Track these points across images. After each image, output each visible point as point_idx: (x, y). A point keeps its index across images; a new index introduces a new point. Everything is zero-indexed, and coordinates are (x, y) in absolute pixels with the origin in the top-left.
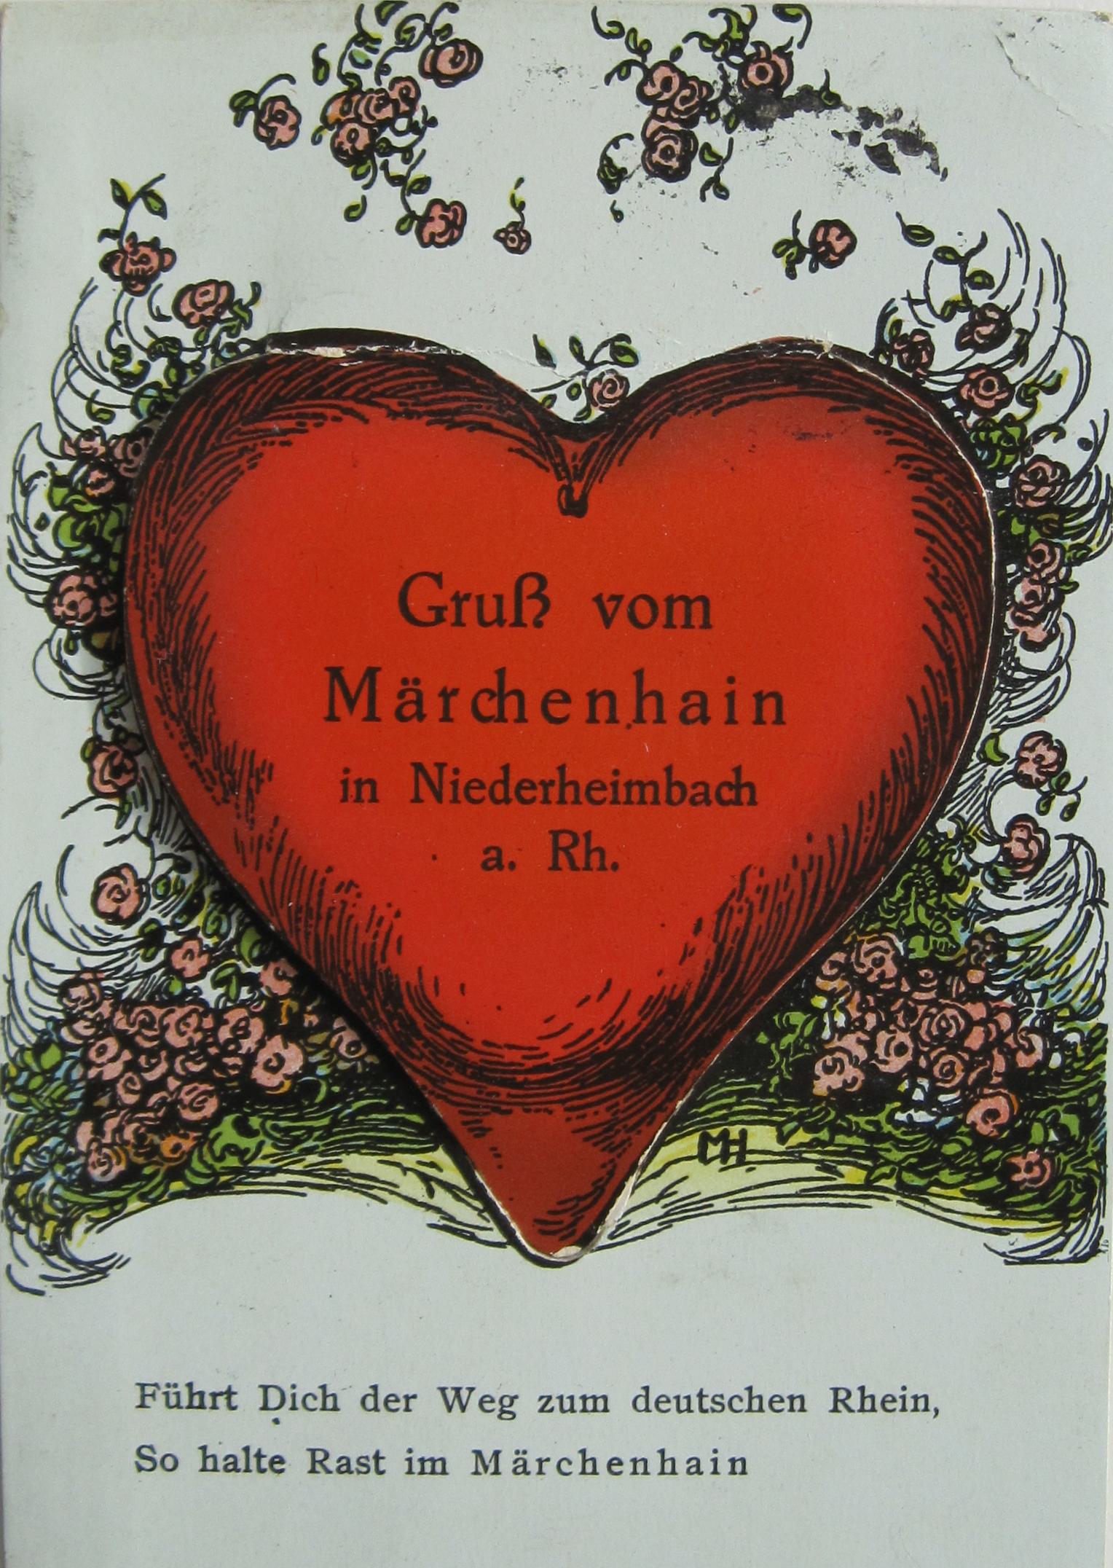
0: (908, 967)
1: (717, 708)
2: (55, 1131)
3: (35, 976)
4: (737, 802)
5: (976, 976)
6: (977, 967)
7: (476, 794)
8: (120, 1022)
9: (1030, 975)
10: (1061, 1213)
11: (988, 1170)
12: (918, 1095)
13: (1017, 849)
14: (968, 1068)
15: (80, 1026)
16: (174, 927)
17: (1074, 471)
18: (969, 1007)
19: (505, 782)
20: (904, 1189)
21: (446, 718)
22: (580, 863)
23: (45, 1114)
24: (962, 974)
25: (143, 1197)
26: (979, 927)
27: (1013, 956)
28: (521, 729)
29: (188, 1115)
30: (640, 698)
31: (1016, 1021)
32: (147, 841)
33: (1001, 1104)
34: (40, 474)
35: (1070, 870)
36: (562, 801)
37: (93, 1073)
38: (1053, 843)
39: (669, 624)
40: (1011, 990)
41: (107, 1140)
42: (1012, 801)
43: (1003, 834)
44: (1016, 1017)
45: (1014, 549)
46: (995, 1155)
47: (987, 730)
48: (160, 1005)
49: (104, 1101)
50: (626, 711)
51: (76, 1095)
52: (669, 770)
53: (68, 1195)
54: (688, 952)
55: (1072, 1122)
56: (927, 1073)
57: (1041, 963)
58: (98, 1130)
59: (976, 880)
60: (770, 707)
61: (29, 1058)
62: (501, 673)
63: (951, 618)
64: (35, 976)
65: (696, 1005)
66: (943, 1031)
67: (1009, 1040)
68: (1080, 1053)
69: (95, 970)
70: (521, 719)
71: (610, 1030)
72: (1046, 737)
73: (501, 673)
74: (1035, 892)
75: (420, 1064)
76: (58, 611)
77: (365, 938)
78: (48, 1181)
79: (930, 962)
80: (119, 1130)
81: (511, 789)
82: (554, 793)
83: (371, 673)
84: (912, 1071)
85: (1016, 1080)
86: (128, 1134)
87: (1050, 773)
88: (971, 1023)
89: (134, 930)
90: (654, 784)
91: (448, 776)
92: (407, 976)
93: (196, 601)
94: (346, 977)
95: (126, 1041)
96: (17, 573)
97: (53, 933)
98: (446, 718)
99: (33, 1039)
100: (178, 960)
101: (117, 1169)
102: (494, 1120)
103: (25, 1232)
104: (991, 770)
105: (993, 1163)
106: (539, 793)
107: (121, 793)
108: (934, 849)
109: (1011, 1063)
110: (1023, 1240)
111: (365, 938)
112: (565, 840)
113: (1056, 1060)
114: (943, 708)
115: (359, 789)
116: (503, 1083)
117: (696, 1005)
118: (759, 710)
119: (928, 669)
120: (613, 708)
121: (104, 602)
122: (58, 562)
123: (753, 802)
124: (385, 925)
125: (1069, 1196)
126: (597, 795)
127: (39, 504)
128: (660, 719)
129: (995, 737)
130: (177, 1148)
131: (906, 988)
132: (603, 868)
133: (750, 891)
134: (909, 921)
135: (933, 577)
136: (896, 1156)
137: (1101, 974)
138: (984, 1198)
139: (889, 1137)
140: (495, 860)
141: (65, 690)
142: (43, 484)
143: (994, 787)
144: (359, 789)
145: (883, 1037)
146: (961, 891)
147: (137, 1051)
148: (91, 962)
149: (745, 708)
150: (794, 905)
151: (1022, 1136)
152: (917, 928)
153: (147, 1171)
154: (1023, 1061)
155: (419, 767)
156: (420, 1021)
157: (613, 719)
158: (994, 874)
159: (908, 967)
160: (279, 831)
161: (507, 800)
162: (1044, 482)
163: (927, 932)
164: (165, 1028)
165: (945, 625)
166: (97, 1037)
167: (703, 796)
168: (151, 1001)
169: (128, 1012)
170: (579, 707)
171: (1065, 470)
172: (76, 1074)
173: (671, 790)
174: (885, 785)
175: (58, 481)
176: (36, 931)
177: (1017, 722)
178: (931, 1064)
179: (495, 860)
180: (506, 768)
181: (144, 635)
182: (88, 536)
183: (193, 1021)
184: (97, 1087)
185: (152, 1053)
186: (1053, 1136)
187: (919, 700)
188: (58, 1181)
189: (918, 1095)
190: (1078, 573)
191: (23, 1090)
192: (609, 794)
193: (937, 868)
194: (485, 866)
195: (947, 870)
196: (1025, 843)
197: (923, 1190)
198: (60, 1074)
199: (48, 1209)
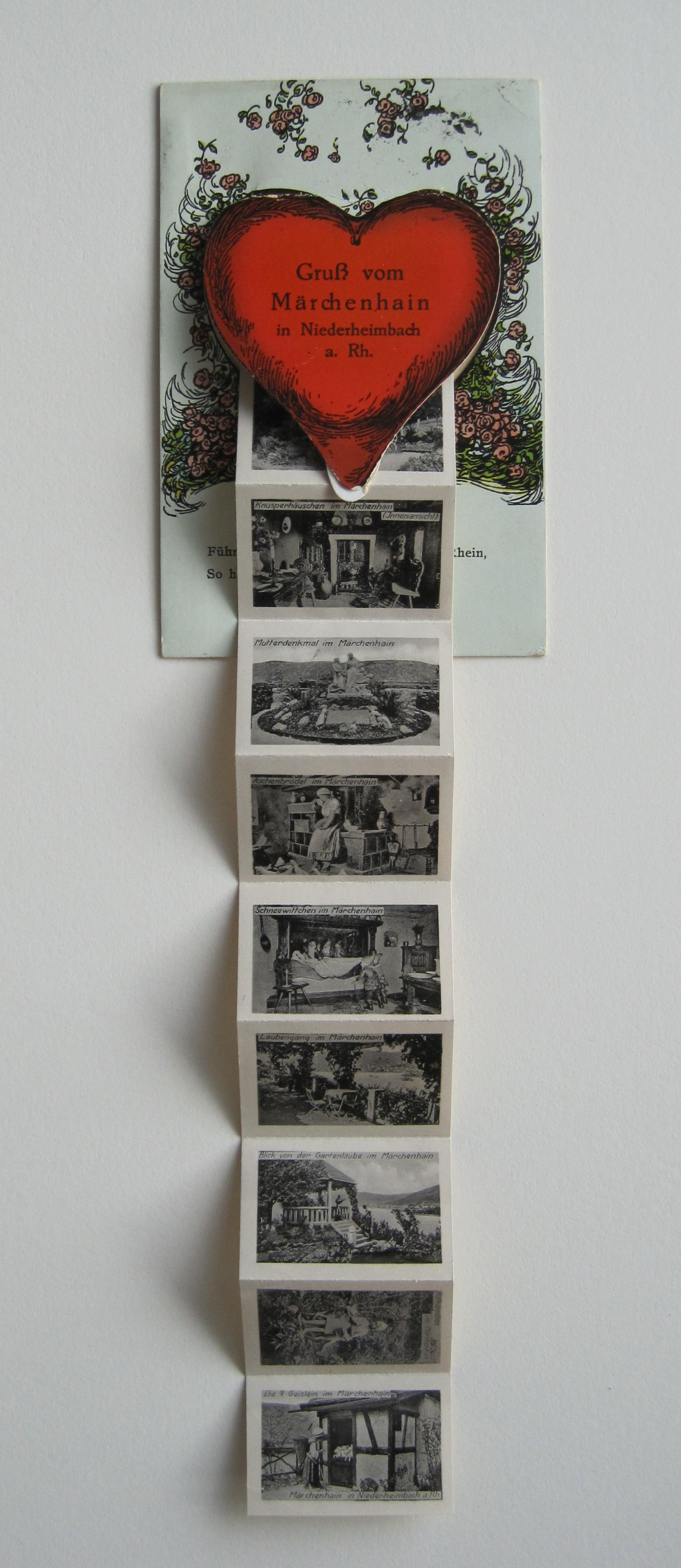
0: (472, 401)
1: (406, 305)
2: (181, 459)
3: (174, 406)
4: (413, 334)
5: (496, 405)
6: (496, 401)
7: (324, 332)
8: (203, 422)
9: (515, 404)
10: (528, 487)
11: (501, 472)
12: (477, 446)
13: (509, 361)
14: (494, 436)
15: (189, 423)
16: (222, 389)
17: (527, 233)
18: (493, 415)
19: (333, 328)
20: (472, 478)
21: (313, 308)
22: (359, 354)
23: (177, 454)
24: (491, 403)
25: (210, 482)
26: (497, 387)
27: (509, 398)
28: (339, 312)
29: (226, 453)
30: (379, 301)
31: (510, 420)
32: (212, 361)
33: (506, 449)
34: (175, 239)
35: (528, 368)
36: (353, 334)
37: (194, 439)
38: (522, 359)
39: (389, 278)
40: (508, 409)
41: (199, 462)
42: (508, 345)
43: (504, 355)
44: (510, 418)
45: (507, 259)
46: (504, 466)
47: (498, 320)
48: (217, 416)
49: (197, 449)
50: (374, 305)
51: (188, 447)
52: (389, 324)
53: (185, 482)
54: (397, 384)
55: (531, 455)
56: (480, 438)
57: (519, 400)
58: (195, 459)
59: (495, 372)
60: (424, 304)
61: (172, 434)
62: (332, 294)
63: (486, 276)
64: (174, 406)
65: (400, 401)
66: (485, 423)
67: (508, 427)
68: (533, 431)
69: (194, 404)
70: (339, 308)
71: (370, 410)
72: (519, 323)
73: (332, 294)
74: (516, 375)
75: (304, 422)
76: (182, 284)
77: (285, 379)
78: (178, 477)
79: (480, 400)
80: (202, 459)
81: (335, 331)
82: (350, 332)
83: (287, 295)
84: (474, 437)
85: (511, 440)
86: (206, 460)
87: (520, 335)
88: (495, 421)
89: (207, 391)
90: (385, 329)
91: (314, 327)
92: (300, 391)
93: (228, 273)
94: (279, 392)
95: (205, 428)
96: (167, 272)
97: (181, 392)
98: (313, 308)
99: (173, 428)
100: (223, 401)
101: (202, 472)
102: (329, 441)
103: (170, 495)
104: (500, 334)
105: (503, 469)
106: (345, 332)
107: (203, 345)
108: (481, 361)
109: (509, 434)
110: (515, 496)
111: (285, 379)
112: (354, 347)
113: (524, 433)
114: (484, 305)
115: (284, 331)
116: (333, 428)
117: (400, 401)
118: (420, 305)
119: (478, 292)
120: (370, 305)
121: (197, 281)
122: (181, 268)
123: (418, 334)
124: (292, 376)
125: (530, 481)
126: (365, 332)
127: (175, 249)
128: (386, 308)
129: (501, 323)
130: (222, 465)
131: (472, 408)
132: (367, 356)
133: (418, 363)
134: (473, 386)
135: (479, 263)
136: (469, 467)
137: (540, 404)
138: (500, 481)
139: (467, 460)
140: (330, 353)
141: (184, 310)
142: (176, 242)
143: (501, 340)
144: (284, 331)
145: (464, 425)
146: (490, 375)
147: (209, 431)
148: (193, 401)
149: (415, 305)
150: (434, 368)
151: (513, 460)
152: (475, 388)
153: (212, 473)
154: (513, 434)
155: (304, 324)
156: (304, 407)
157: (370, 308)
158: (502, 369)
159: (472, 401)
160: (256, 346)
161: (334, 334)
162: (515, 237)
163: (479, 390)
164: (218, 424)
165: (484, 279)
166: (195, 427)
167: (402, 332)
168: (213, 415)
169: (206, 418)
170: (358, 305)
171: (524, 233)
172: (188, 440)
173: (391, 331)
174: (464, 329)
175: (181, 241)
176: (174, 391)
177: (509, 318)
178: (481, 435)
179: (330, 353)
180: (334, 324)
181: (210, 284)
182: (191, 259)
183: (228, 421)
184: (195, 444)
185: (213, 432)
186: (524, 460)
187: (475, 302)
188: (182, 477)
189: (477, 446)
190: (529, 267)
191: (170, 446)
192: (369, 332)
193: (482, 367)
194: (327, 356)
195: (485, 368)
196: (512, 359)
197: (479, 478)
198: (182, 440)
199: (178, 486)
